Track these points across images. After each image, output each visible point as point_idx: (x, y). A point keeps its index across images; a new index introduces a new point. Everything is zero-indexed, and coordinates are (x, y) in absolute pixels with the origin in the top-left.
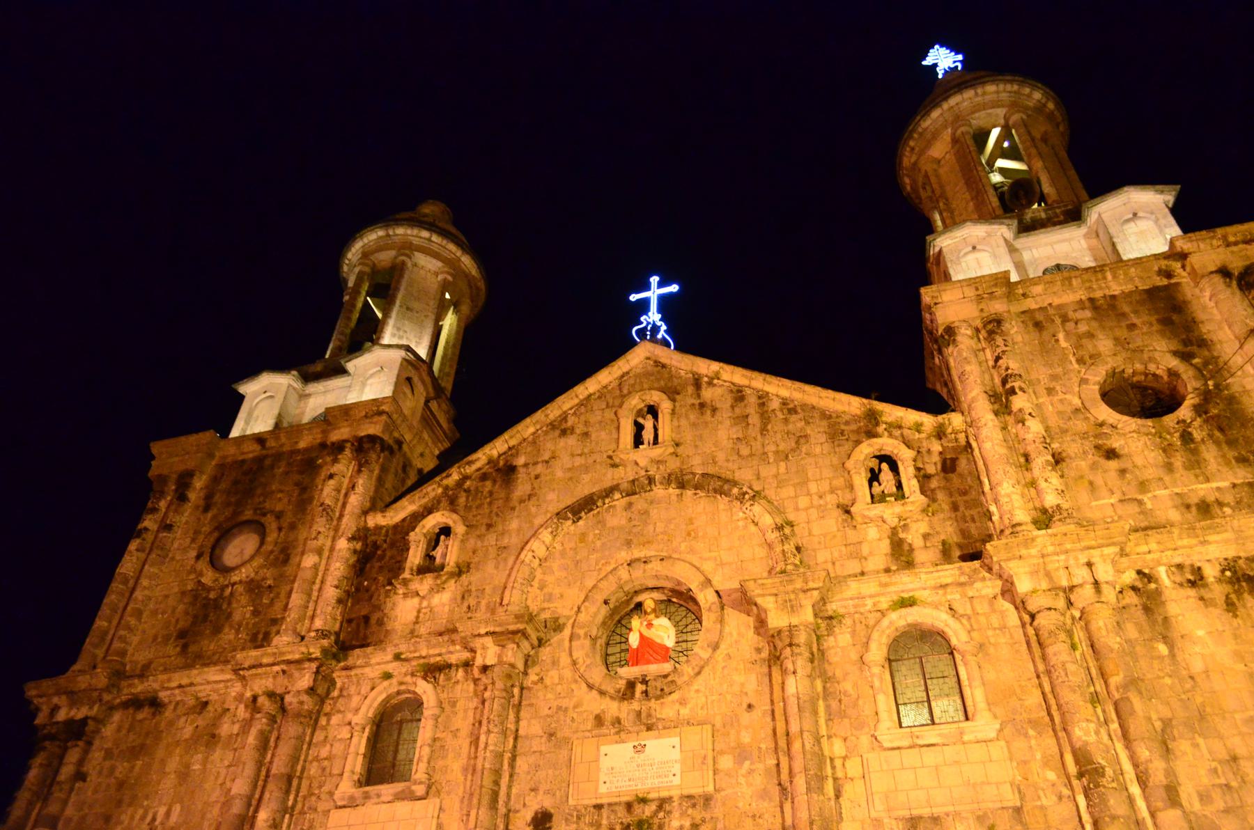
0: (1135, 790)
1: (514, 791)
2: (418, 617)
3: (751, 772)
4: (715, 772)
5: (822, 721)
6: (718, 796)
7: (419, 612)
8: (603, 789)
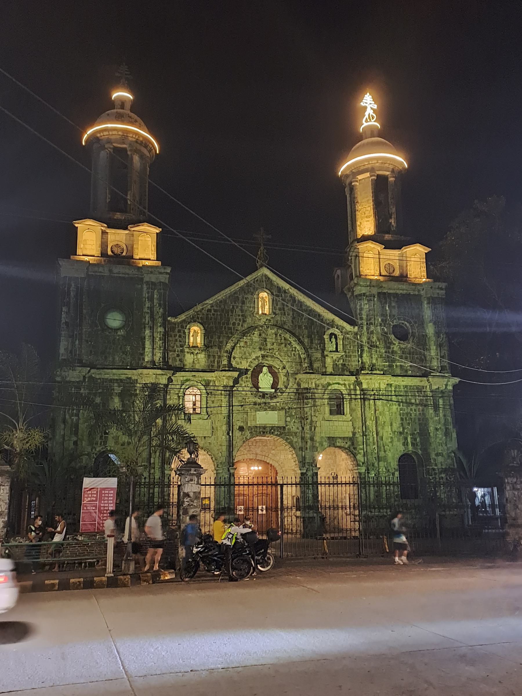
0: (375, 436)
1: (233, 420)
2: (194, 362)
3: (294, 422)
4: (286, 421)
5: (312, 412)
6: (287, 427)
7: (194, 359)
8: (258, 423)
